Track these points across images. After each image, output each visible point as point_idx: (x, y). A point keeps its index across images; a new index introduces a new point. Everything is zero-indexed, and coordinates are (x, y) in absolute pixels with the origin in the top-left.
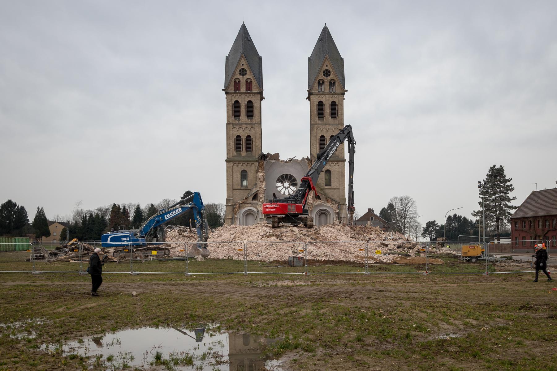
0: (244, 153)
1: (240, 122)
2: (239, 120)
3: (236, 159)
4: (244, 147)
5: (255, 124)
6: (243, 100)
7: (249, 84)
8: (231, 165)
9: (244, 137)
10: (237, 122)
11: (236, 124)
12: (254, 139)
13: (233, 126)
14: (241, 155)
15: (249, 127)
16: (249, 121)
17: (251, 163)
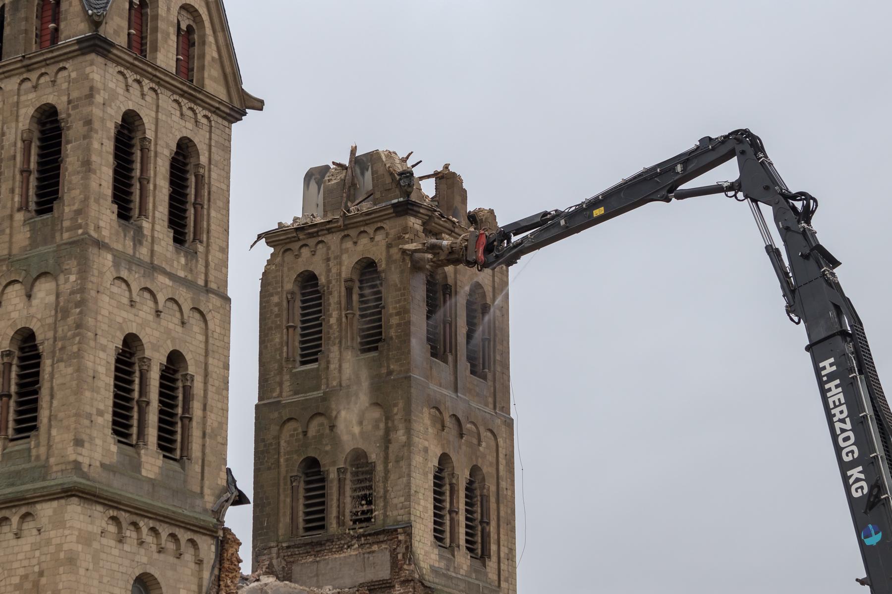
0: (152, 462)
1: (144, 252)
2: (138, 237)
3: (118, 486)
4: (153, 417)
5: (207, 289)
6: (167, 124)
7: (188, 39)
8: (96, 530)
9: (156, 358)
10: (129, 243)
11: (133, 262)
12: (198, 386)
13: (116, 264)
14: (137, 466)
15: (185, 297)
16: (178, 264)
17: (184, 536)
